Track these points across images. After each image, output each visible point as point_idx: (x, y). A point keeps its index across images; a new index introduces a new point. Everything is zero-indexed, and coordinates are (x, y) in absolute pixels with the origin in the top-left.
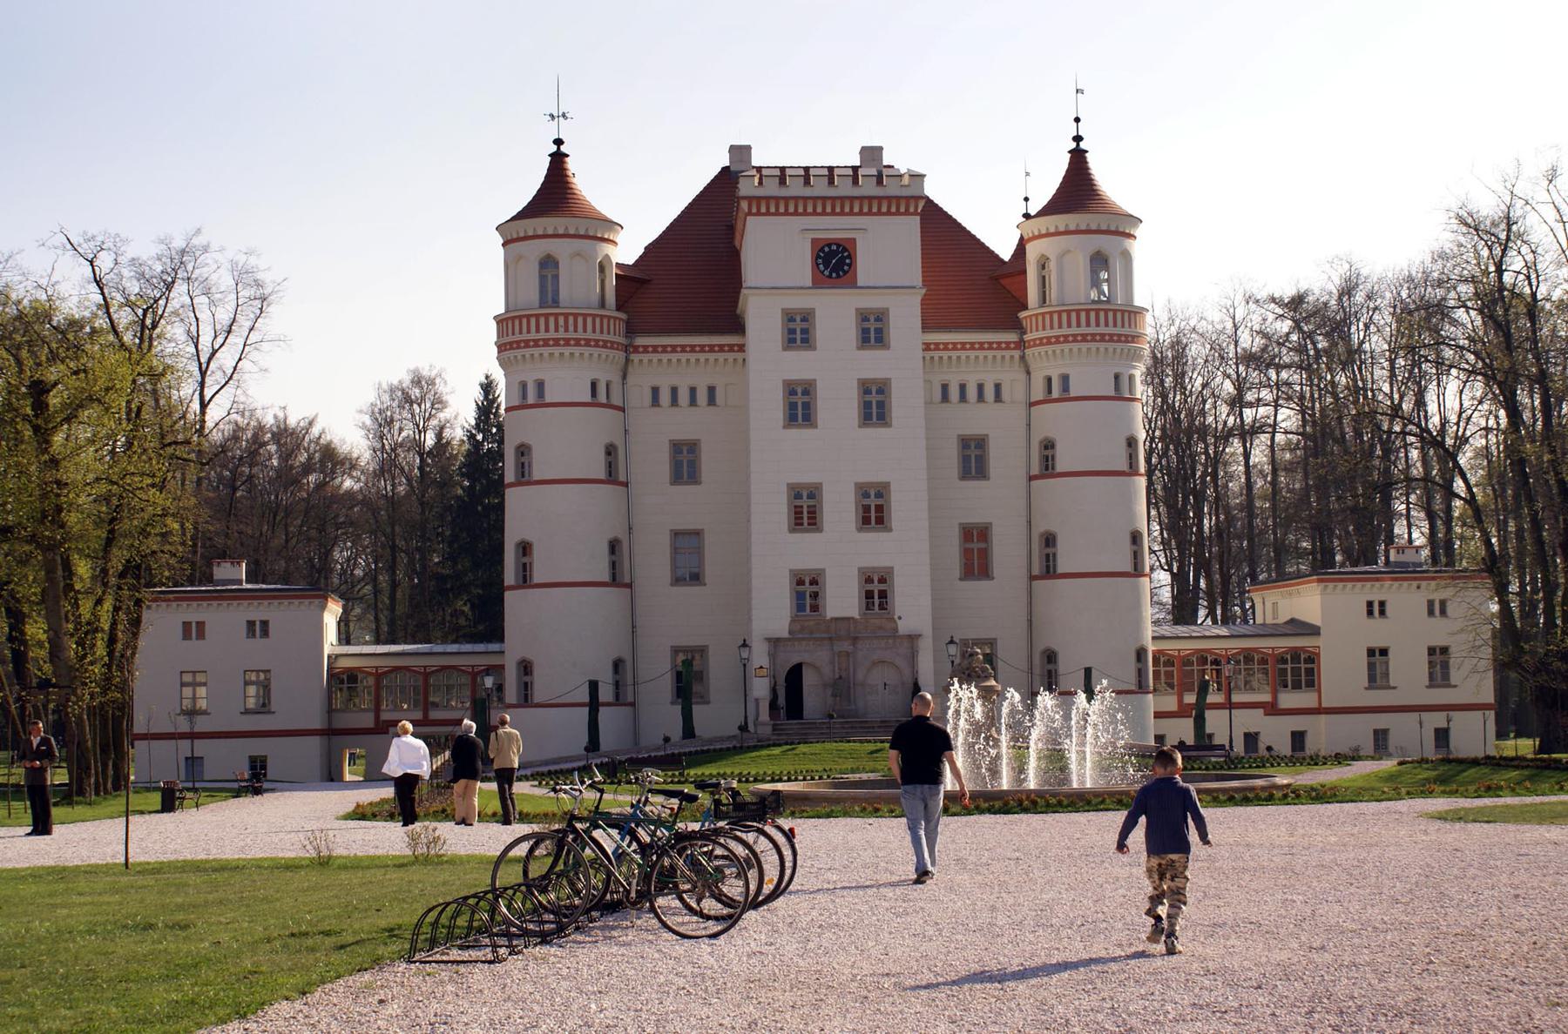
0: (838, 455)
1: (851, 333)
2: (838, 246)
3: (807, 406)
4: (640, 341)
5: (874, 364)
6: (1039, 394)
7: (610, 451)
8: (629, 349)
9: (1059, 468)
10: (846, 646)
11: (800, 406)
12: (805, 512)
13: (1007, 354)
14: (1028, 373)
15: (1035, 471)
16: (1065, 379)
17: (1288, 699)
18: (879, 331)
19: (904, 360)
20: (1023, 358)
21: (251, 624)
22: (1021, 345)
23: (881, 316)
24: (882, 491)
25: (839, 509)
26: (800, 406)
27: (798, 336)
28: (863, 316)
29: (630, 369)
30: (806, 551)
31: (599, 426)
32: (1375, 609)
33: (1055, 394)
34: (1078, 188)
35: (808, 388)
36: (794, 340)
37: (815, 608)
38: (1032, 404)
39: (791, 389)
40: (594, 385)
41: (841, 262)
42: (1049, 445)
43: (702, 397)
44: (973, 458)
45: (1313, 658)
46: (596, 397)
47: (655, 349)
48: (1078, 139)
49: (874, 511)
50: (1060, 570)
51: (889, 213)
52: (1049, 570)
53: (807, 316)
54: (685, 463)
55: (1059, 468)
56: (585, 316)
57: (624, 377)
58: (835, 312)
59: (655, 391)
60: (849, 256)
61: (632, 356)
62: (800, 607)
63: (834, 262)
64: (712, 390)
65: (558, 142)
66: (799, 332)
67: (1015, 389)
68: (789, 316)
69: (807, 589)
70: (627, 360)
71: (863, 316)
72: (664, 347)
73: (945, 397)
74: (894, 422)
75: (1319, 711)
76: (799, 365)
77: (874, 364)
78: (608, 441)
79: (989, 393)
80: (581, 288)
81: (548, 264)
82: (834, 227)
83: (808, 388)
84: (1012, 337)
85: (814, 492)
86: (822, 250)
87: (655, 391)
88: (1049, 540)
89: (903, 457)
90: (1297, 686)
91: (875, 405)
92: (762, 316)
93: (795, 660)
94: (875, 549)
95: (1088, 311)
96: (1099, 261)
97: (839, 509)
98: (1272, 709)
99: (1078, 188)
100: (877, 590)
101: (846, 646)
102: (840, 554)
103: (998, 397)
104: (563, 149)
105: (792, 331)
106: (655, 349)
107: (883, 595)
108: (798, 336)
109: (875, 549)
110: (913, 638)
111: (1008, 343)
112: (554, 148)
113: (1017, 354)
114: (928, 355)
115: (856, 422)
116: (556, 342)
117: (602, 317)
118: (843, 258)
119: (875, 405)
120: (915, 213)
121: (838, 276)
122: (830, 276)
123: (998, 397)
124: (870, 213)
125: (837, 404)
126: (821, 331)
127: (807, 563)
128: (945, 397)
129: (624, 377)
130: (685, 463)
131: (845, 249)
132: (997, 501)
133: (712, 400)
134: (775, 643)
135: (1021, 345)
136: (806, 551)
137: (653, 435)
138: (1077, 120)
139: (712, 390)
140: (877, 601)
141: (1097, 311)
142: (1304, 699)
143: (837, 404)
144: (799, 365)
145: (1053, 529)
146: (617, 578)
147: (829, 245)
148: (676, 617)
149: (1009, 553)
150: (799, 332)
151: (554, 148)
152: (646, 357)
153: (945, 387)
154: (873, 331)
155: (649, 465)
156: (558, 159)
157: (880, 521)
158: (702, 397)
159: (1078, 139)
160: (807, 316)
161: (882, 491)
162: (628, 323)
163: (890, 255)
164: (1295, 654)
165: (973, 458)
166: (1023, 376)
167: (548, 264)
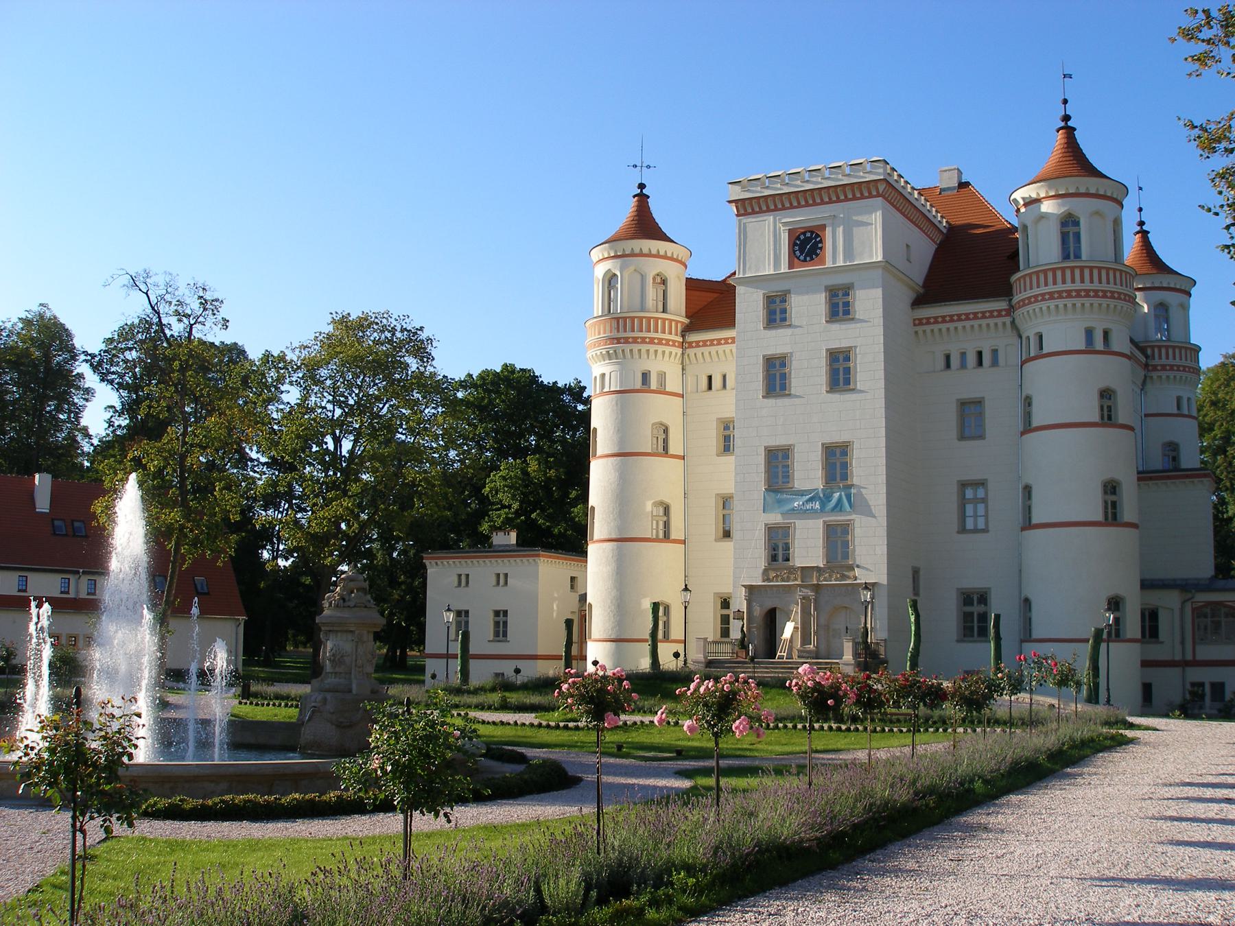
2: (812, 232)
4: (693, 337)
5: (840, 336)
9: (1035, 424)
11: (776, 376)
13: (999, 321)
14: (1020, 337)
20: (1013, 322)
36: (775, 321)
38: (1023, 363)
44: (970, 416)
47: (705, 343)
48: (1066, 118)
50: (1035, 521)
52: (1028, 525)
55: (1035, 424)
60: (821, 241)
61: (691, 352)
62: (774, 558)
63: (806, 245)
65: (642, 186)
66: (776, 314)
68: (770, 300)
72: (712, 341)
73: (948, 366)
76: (778, 341)
77: (840, 336)
79: (987, 359)
84: (1001, 305)
86: (798, 238)
88: (1028, 490)
91: (840, 370)
92: (749, 304)
93: (769, 605)
95: (1054, 270)
103: (995, 363)
106: (705, 343)
108: (778, 317)
111: (999, 311)
113: (1008, 320)
114: (920, 329)
115: (824, 388)
118: (816, 243)
119: (840, 370)
120: (878, 195)
121: (812, 259)
122: (805, 260)
123: (995, 363)
125: (809, 373)
128: (948, 366)
131: (818, 236)
134: (751, 589)
135: (1011, 310)
138: (1065, 102)
141: (1063, 269)
143: (809, 373)
144: (778, 341)
145: (1030, 482)
147: (804, 233)
150: (776, 314)
152: (699, 351)
153: (948, 357)
154: (839, 307)
156: (642, 198)
159: (1066, 118)
163: (865, 239)
166: (1016, 341)
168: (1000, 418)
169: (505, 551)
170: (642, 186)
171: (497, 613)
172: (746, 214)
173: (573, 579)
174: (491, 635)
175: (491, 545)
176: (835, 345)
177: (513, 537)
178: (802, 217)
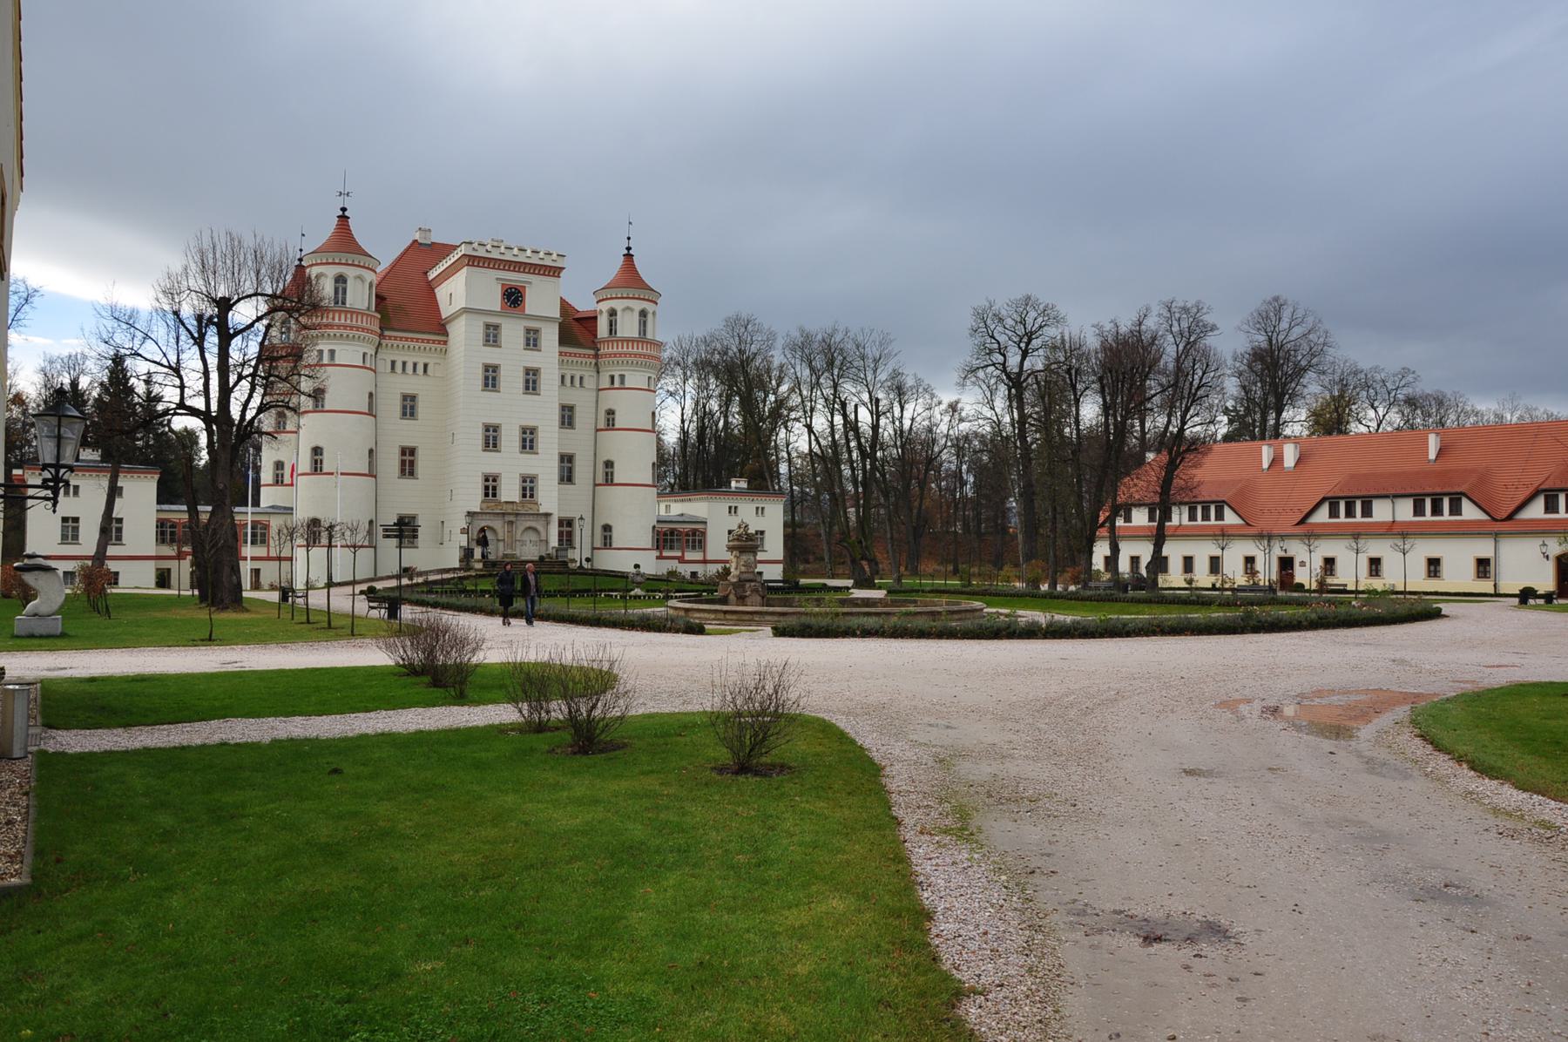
1: (521, 341)
3: (494, 379)
6: (605, 383)
10: (512, 518)
11: (491, 378)
12: (491, 438)
15: (602, 425)
16: (622, 377)
17: (689, 556)
18: (535, 340)
19: (549, 355)
22: (596, 356)
23: (536, 331)
25: (510, 439)
26: (491, 378)
28: (528, 331)
30: (491, 463)
31: (364, 380)
32: (733, 510)
33: (617, 384)
34: (630, 278)
35: (495, 368)
37: (494, 495)
39: (487, 368)
42: (611, 412)
43: (420, 369)
45: (704, 534)
48: (629, 249)
49: (528, 441)
52: (609, 480)
53: (497, 327)
54: (409, 406)
59: (393, 363)
61: (384, 342)
62: (487, 495)
63: (513, 297)
64: (426, 366)
65: (344, 209)
66: (492, 336)
67: (590, 383)
69: (491, 486)
71: (528, 331)
75: (705, 562)
76: (491, 356)
82: (514, 277)
83: (495, 368)
85: (496, 428)
87: (393, 363)
88: (609, 464)
89: (543, 412)
90: (694, 548)
91: (531, 381)
93: (483, 524)
94: (529, 464)
96: (643, 314)
97: (510, 439)
98: (681, 560)
99: (630, 278)
100: (528, 486)
101: (512, 518)
102: (510, 465)
105: (488, 335)
109: (529, 464)
110: (547, 515)
116: (345, 327)
119: (531, 381)
125: (511, 379)
127: (491, 470)
130: (409, 406)
132: (579, 441)
133: (425, 371)
134: (469, 514)
135: (596, 356)
136: (491, 463)
139: (426, 366)
142: (698, 556)
143: (511, 379)
144: (491, 356)
148: (403, 498)
149: (582, 471)
150: (492, 336)
152: (389, 342)
155: (390, 406)
156: (343, 218)
158: (420, 369)
159: (629, 249)
160: (497, 327)
161: (533, 430)
162: (381, 320)
164: (694, 532)
165: (567, 417)
168: (584, 418)
170: (344, 209)
176: (529, 365)
178: (514, 277)
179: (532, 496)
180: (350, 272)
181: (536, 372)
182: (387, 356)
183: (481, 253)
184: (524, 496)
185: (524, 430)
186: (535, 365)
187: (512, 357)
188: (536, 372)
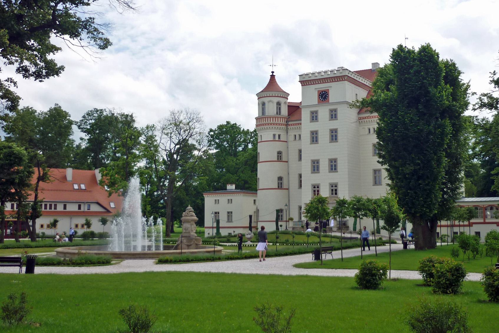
0: (324, 151)
3: (316, 137)
4: (290, 123)
5: (334, 125)
7: (279, 153)
8: (287, 125)
11: (314, 137)
12: (315, 167)
21: (229, 200)
24: (335, 160)
25: (324, 166)
26: (314, 137)
27: (315, 118)
28: (331, 111)
29: (289, 131)
30: (315, 179)
40: (274, 135)
41: (326, 96)
46: (277, 139)
49: (333, 166)
51: (338, 81)
56: (270, 117)
57: (287, 133)
58: (324, 112)
63: (324, 96)
65: (273, 72)
66: (314, 117)
69: (316, 189)
70: (287, 129)
71: (331, 111)
72: (296, 124)
74: (339, 141)
76: (314, 126)
77: (334, 125)
78: (278, 150)
80: (271, 110)
81: (264, 104)
82: (323, 86)
85: (318, 162)
91: (334, 136)
92: (305, 115)
94: (334, 178)
97: (324, 166)
100: (334, 189)
102: (324, 180)
104: (274, 74)
107: (336, 190)
108: (315, 118)
109: (334, 178)
112: (271, 74)
114: (361, 121)
117: (278, 117)
119: (334, 136)
124: (333, 82)
125: (324, 137)
126: (320, 115)
127: (316, 182)
129: (287, 133)
136: (315, 179)
137: (293, 147)
140: (334, 192)
143: (324, 137)
144: (314, 126)
146: (280, 186)
150: (314, 117)
151: (271, 74)
152: (292, 127)
154: (333, 115)
155: (293, 156)
157: (335, 169)
160: (316, 112)
161: (335, 160)
167: (264, 104)
169: (231, 192)
170: (273, 72)
171: (228, 213)
172: (304, 85)
173: (255, 201)
174: (226, 219)
175: (226, 189)
176: (332, 128)
177: (233, 187)
178: (323, 86)
179: (336, 194)
180: (266, 100)
181: (336, 131)
182: (292, 133)
183: (307, 78)
184: (332, 194)
185: (331, 161)
186: (335, 127)
187: (324, 125)
188: (336, 131)
